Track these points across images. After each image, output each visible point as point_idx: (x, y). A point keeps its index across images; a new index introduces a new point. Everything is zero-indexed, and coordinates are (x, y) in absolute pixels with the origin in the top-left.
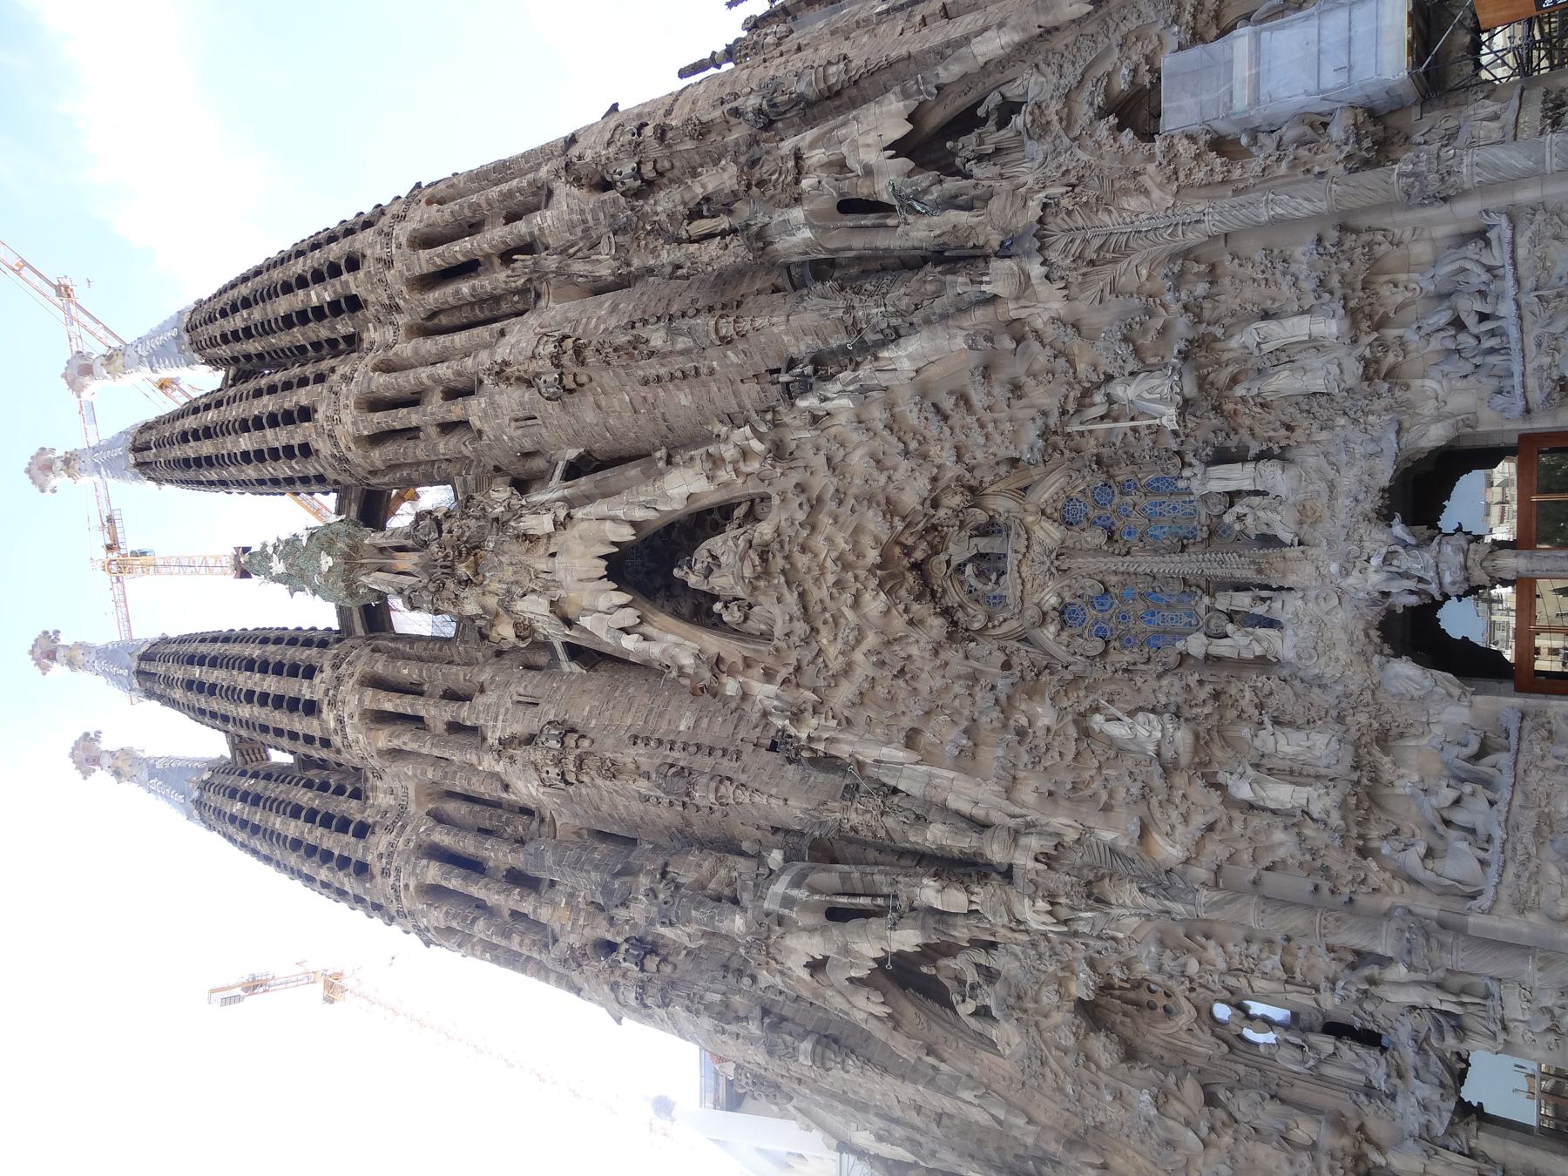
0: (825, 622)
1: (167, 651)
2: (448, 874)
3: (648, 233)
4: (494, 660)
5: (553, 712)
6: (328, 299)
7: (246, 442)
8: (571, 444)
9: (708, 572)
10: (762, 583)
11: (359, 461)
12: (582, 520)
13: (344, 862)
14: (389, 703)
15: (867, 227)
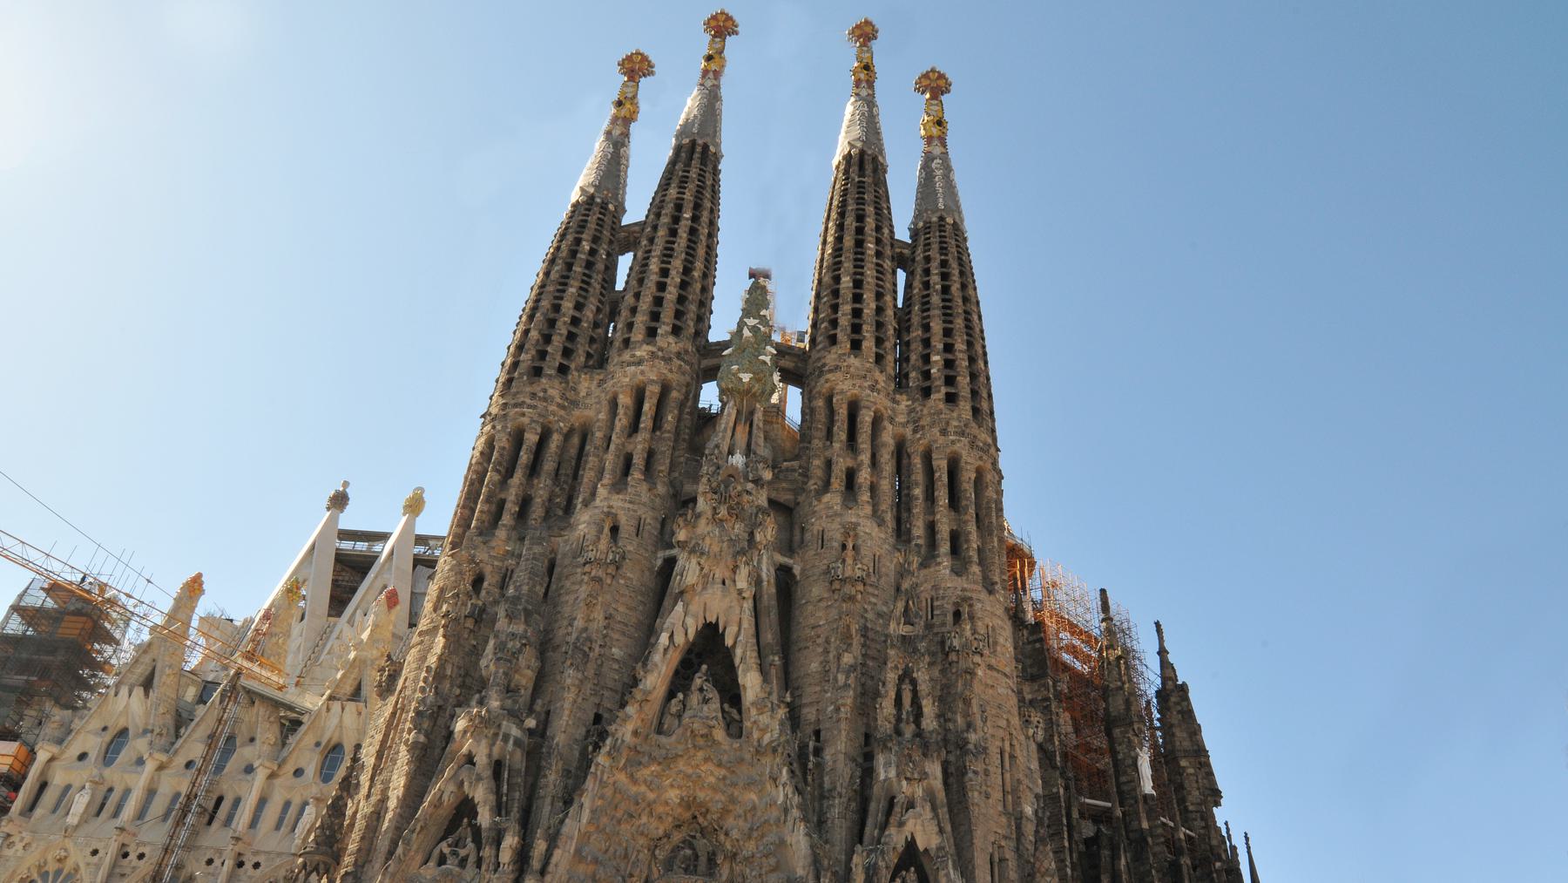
0: (664, 771)
1: (707, 175)
2: (531, 451)
3: (907, 666)
4: (671, 492)
5: (632, 549)
6: (932, 371)
7: (846, 281)
8: (803, 570)
9: (701, 690)
10: (689, 734)
11: (817, 389)
12: (742, 607)
13: (542, 355)
14: (648, 407)
15: (877, 815)
